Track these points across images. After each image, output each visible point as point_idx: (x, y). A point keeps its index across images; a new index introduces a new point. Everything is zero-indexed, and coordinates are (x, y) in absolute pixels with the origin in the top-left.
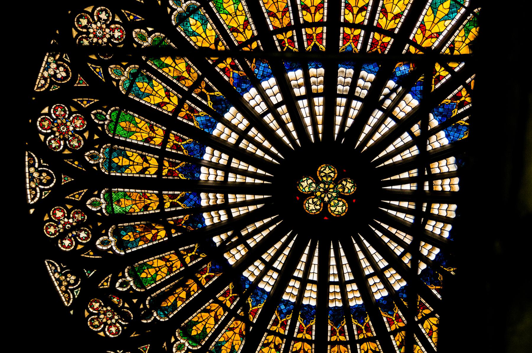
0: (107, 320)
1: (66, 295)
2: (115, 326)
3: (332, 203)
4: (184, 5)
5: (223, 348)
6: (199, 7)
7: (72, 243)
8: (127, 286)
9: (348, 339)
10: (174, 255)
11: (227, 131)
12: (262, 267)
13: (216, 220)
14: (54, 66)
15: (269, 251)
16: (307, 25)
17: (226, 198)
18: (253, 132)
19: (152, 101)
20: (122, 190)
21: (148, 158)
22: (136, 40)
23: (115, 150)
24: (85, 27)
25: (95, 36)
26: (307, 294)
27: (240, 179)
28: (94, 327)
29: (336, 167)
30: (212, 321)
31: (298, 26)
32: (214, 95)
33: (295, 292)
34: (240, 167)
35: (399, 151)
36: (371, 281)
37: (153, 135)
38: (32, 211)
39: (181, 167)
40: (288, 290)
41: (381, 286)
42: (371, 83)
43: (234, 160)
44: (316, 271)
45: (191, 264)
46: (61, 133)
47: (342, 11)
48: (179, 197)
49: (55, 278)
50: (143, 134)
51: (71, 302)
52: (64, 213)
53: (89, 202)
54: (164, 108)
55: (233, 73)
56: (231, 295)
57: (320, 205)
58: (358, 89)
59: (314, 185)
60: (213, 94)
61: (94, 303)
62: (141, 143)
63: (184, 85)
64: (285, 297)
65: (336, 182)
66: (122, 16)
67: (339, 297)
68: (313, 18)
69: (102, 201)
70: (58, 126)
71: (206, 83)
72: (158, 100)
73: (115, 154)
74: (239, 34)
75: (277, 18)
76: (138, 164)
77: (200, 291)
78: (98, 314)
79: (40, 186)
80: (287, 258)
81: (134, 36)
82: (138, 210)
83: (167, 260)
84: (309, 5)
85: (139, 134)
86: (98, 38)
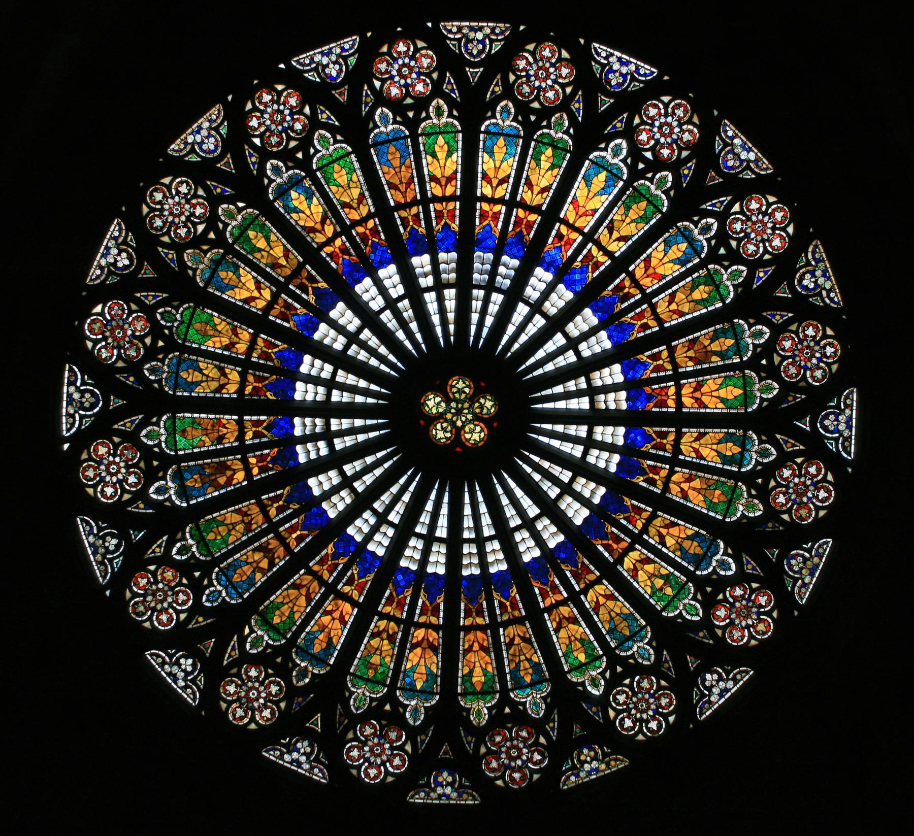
0: (157, 604)
1: (102, 568)
2: (167, 613)
3: (467, 429)
4: (286, 175)
5: (316, 641)
6: (304, 178)
7: (116, 492)
8: (186, 554)
9: (488, 622)
10: (254, 506)
11: (332, 333)
12: (372, 521)
13: (313, 456)
14: (114, 251)
15: (383, 498)
16: (435, 199)
17: (328, 424)
18: (366, 334)
19: (237, 296)
20: (189, 415)
21: (227, 371)
22: (223, 218)
23: (185, 360)
24: (160, 203)
25: (171, 213)
26: (432, 558)
27: (346, 397)
28: (138, 614)
29: (472, 379)
30: (302, 601)
31: (425, 201)
32: (318, 288)
33: (417, 556)
34: (348, 382)
35: (551, 357)
36: (518, 537)
37: (235, 339)
38: (66, 446)
39: (271, 383)
40: (408, 552)
41: (531, 543)
42: (515, 270)
43: (340, 372)
44: (445, 524)
45: (278, 518)
46: (115, 339)
47: (479, 182)
48: (265, 424)
49: (89, 542)
50: (223, 339)
51: (108, 577)
52: (109, 449)
53: (144, 432)
54: (253, 304)
55: (343, 259)
56: (330, 563)
57: (451, 431)
58: (499, 278)
59: (443, 404)
60: (315, 285)
61: (139, 579)
62: (220, 351)
63: (280, 275)
64: (403, 563)
65: (472, 399)
66: (207, 189)
67: (475, 561)
68: (444, 191)
69: (162, 431)
70: (112, 331)
71: (309, 272)
72: (245, 294)
73: (184, 366)
74: (352, 211)
75: (400, 191)
76: (213, 379)
77: (287, 558)
78: (144, 596)
79: (81, 412)
80: (406, 507)
81: (220, 212)
82: (210, 443)
83: (245, 514)
84: (439, 176)
85: (218, 339)
86: (175, 216)
